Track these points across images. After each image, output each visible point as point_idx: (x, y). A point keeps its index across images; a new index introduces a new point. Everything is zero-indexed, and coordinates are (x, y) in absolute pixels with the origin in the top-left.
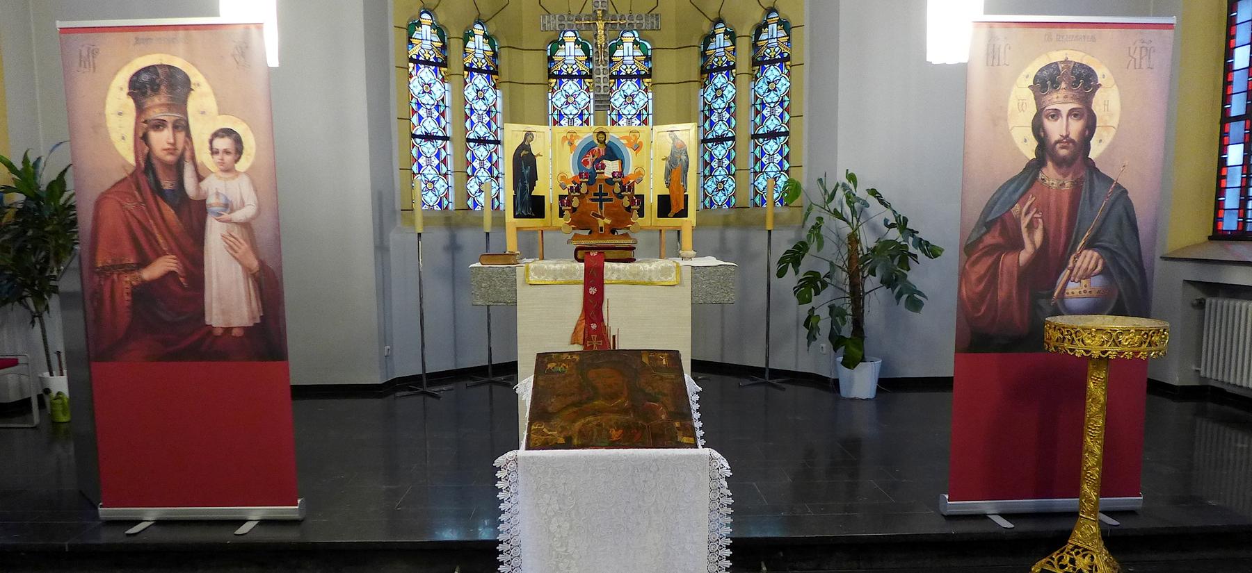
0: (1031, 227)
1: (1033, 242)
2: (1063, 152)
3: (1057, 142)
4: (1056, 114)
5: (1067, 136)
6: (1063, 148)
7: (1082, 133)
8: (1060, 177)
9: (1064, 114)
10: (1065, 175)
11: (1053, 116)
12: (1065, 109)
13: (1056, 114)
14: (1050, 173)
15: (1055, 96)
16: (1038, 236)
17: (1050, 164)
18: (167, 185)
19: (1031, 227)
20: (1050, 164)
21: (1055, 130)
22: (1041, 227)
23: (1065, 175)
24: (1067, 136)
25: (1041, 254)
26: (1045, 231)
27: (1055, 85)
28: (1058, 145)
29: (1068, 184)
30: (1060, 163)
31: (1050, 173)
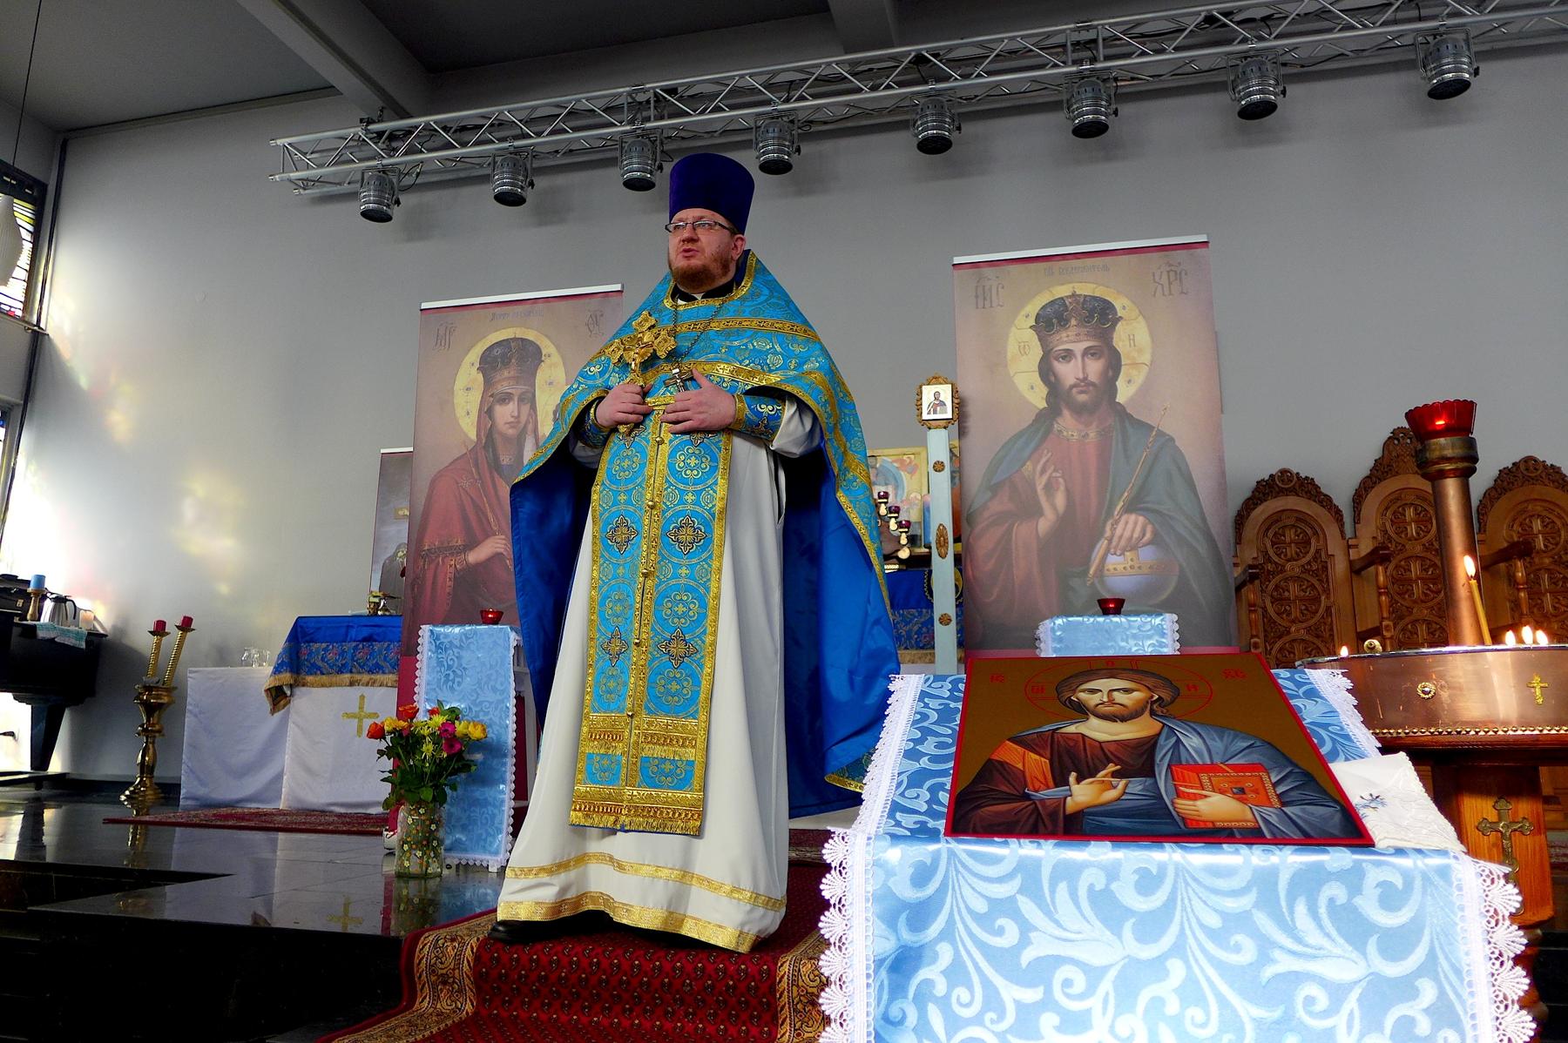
0: (1049, 488)
2: (1082, 398)
5: (1085, 379)
6: (1081, 392)
7: (1104, 373)
8: (1081, 427)
12: (1079, 348)
18: (505, 460)
24: (1085, 379)
29: (1092, 435)
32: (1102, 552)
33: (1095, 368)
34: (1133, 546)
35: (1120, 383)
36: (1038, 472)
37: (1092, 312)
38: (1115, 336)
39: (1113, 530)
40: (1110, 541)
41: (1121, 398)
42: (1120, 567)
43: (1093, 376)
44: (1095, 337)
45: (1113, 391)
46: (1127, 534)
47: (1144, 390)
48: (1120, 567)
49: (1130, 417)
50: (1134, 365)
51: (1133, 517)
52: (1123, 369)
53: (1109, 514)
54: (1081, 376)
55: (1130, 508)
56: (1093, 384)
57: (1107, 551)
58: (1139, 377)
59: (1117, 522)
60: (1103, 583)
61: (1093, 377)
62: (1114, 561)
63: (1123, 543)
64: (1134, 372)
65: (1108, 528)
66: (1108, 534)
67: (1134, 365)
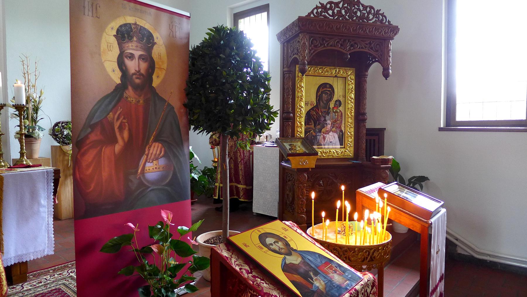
1: (123, 138)
2: (137, 81)
3: (134, 74)
4: (131, 57)
5: (139, 71)
6: (137, 78)
8: (136, 96)
9: (137, 57)
10: (140, 96)
11: (130, 57)
12: (137, 53)
13: (131, 57)
14: (130, 93)
15: (130, 45)
16: (126, 134)
21: (132, 66)
22: (127, 128)
23: (140, 96)
24: (139, 71)
25: (128, 145)
26: (130, 130)
27: (130, 38)
28: (134, 76)
29: (141, 101)
30: (136, 88)
31: (130, 93)
32: (144, 161)
33: (144, 66)
34: (157, 159)
35: (154, 77)
36: (115, 118)
37: (143, 36)
38: (153, 52)
39: (149, 150)
40: (147, 155)
41: (154, 84)
42: (151, 168)
43: (143, 71)
45: (151, 80)
46: (154, 152)
47: (164, 82)
48: (151, 168)
50: (160, 69)
51: (157, 144)
52: (156, 69)
54: (137, 69)
55: (156, 140)
56: (142, 75)
57: (146, 161)
58: (162, 76)
59: (151, 146)
60: (144, 176)
61: (143, 71)
62: (148, 165)
63: (153, 156)
64: (160, 73)
66: (146, 152)
67: (160, 69)
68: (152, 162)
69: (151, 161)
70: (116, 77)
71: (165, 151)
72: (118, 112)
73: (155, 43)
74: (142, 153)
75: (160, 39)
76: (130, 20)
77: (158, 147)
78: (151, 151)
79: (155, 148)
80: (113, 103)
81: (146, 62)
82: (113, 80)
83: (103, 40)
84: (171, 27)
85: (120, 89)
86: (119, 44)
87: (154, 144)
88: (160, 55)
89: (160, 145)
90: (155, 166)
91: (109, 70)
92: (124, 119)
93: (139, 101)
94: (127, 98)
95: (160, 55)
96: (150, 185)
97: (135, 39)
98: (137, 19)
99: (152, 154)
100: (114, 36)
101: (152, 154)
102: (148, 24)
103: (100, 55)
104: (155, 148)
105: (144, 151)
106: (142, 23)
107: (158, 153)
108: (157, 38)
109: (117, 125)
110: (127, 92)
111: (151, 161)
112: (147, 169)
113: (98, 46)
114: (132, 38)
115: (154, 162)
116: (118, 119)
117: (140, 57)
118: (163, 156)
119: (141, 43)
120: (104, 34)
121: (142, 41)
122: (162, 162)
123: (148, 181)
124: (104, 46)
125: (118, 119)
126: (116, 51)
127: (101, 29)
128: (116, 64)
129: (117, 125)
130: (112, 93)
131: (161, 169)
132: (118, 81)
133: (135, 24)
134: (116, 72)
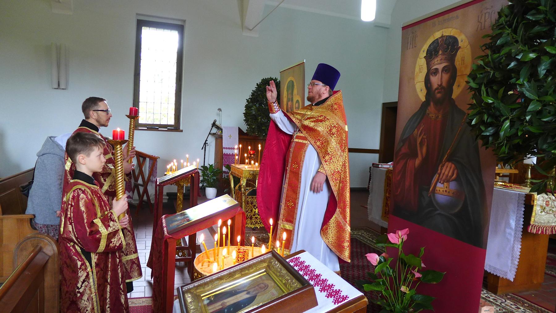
3: (436, 89)
6: (438, 93)
9: (440, 71)
11: (434, 73)
12: (440, 67)
13: (436, 71)
14: (432, 109)
15: (436, 60)
17: (432, 104)
19: (422, 143)
20: (432, 104)
21: (435, 80)
22: (426, 144)
24: (441, 84)
26: (428, 146)
27: (436, 52)
29: (440, 117)
30: (438, 103)
31: (432, 109)
32: (436, 180)
34: (448, 181)
35: (455, 87)
38: (456, 59)
39: (441, 169)
41: (454, 96)
42: (441, 190)
43: (444, 84)
44: (447, 60)
46: (446, 173)
48: (441, 190)
49: (456, 106)
51: (450, 164)
53: (441, 161)
56: (443, 88)
59: (443, 166)
60: (434, 196)
61: (444, 84)
62: (439, 185)
65: (440, 168)
66: (439, 172)
67: (462, 75)
68: (443, 183)
69: (442, 182)
70: (422, 96)
71: (458, 174)
72: (421, 129)
73: (460, 47)
74: (434, 172)
75: (463, 40)
76: (438, 35)
77: (451, 168)
78: (443, 171)
79: (448, 169)
80: (418, 120)
81: (447, 73)
82: (419, 98)
83: (417, 64)
84: (480, 19)
85: (425, 106)
86: (427, 64)
87: (447, 163)
88: (463, 60)
89: (453, 166)
90: (445, 189)
91: (418, 90)
92: (424, 135)
93: (438, 116)
94: (428, 114)
95: (463, 60)
96: (438, 208)
97: (440, 52)
98: (444, 30)
99: (444, 174)
100: (425, 57)
101: (444, 174)
102: (454, 30)
103: (414, 79)
104: (448, 169)
105: (438, 170)
106: (448, 32)
107: (450, 174)
108: (462, 41)
109: (419, 140)
110: (429, 108)
111: (442, 182)
112: (438, 189)
113: (413, 72)
114: (438, 52)
115: (445, 184)
116: (420, 135)
117: (444, 69)
118: (455, 180)
119: (445, 55)
120: (418, 59)
121: (446, 52)
122: (453, 186)
123: (438, 203)
124: (417, 69)
125: (420, 135)
126: (425, 71)
127: (416, 56)
128: (424, 83)
129: (419, 140)
130: (418, 111)
131: (451, 194)
132: (423, 99)
133: (442, 36)
134: (423, 91)
